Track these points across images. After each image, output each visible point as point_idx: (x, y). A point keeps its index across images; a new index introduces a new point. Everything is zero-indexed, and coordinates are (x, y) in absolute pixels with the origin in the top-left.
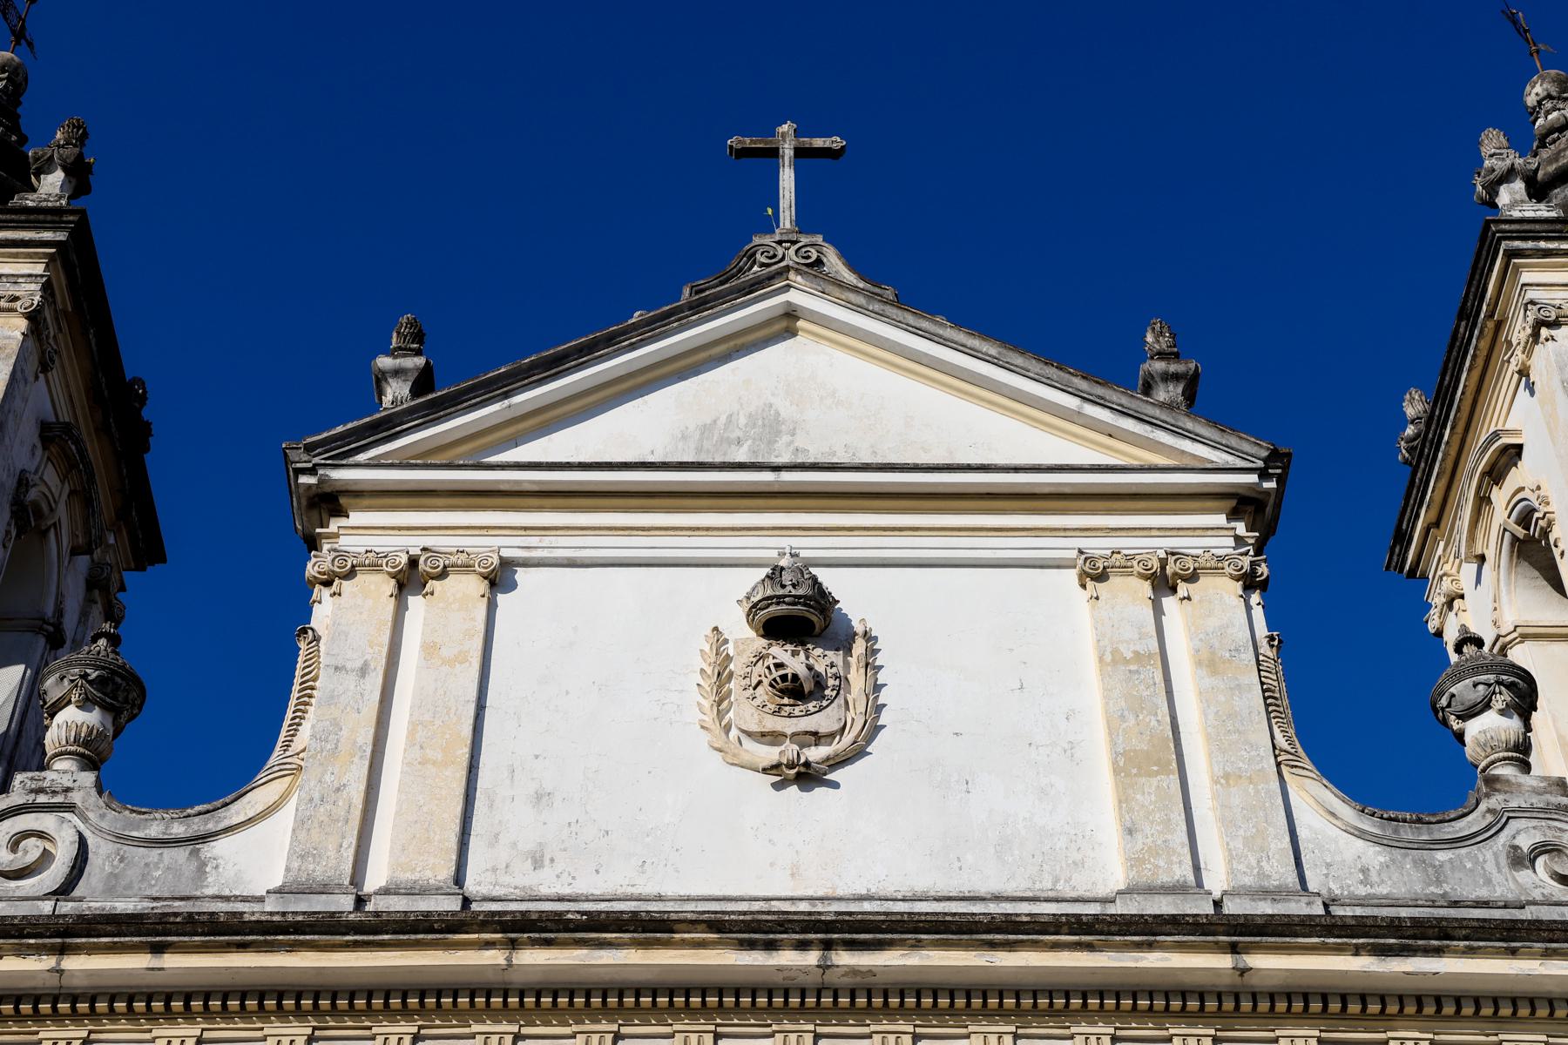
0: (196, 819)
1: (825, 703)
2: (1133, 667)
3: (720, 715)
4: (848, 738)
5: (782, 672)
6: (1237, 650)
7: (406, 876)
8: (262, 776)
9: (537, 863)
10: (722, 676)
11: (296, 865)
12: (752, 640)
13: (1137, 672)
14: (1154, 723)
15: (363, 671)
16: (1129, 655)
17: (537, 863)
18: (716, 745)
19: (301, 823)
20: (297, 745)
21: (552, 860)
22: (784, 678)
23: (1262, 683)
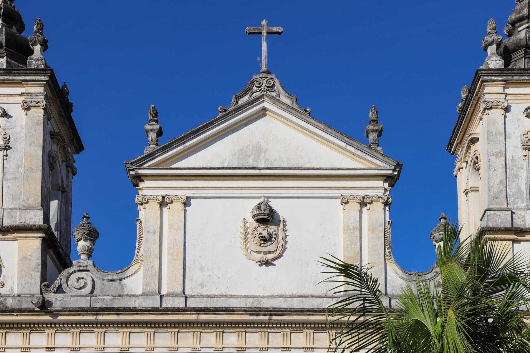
0: (119, 274)
1: (272, 242)
2: (352, 231)
3: (246, 245)
4: (278, 252)
5: (261, 235)
6: (380, 226)
7: (172, 291)
8: (133, 263)
9: (202, 286)
10: (246, 234)
11: (145, 288)
12: (254, 223)
13: (353, 233)
14: (355, 248)
15: (154, 233)
16: (351, 227)
17: (202, 286)
18: (245, 254)
19: (144, 276)
20: (140, 254)
21: (206, 286)
22: (262, 237)
23: (385, 235)
